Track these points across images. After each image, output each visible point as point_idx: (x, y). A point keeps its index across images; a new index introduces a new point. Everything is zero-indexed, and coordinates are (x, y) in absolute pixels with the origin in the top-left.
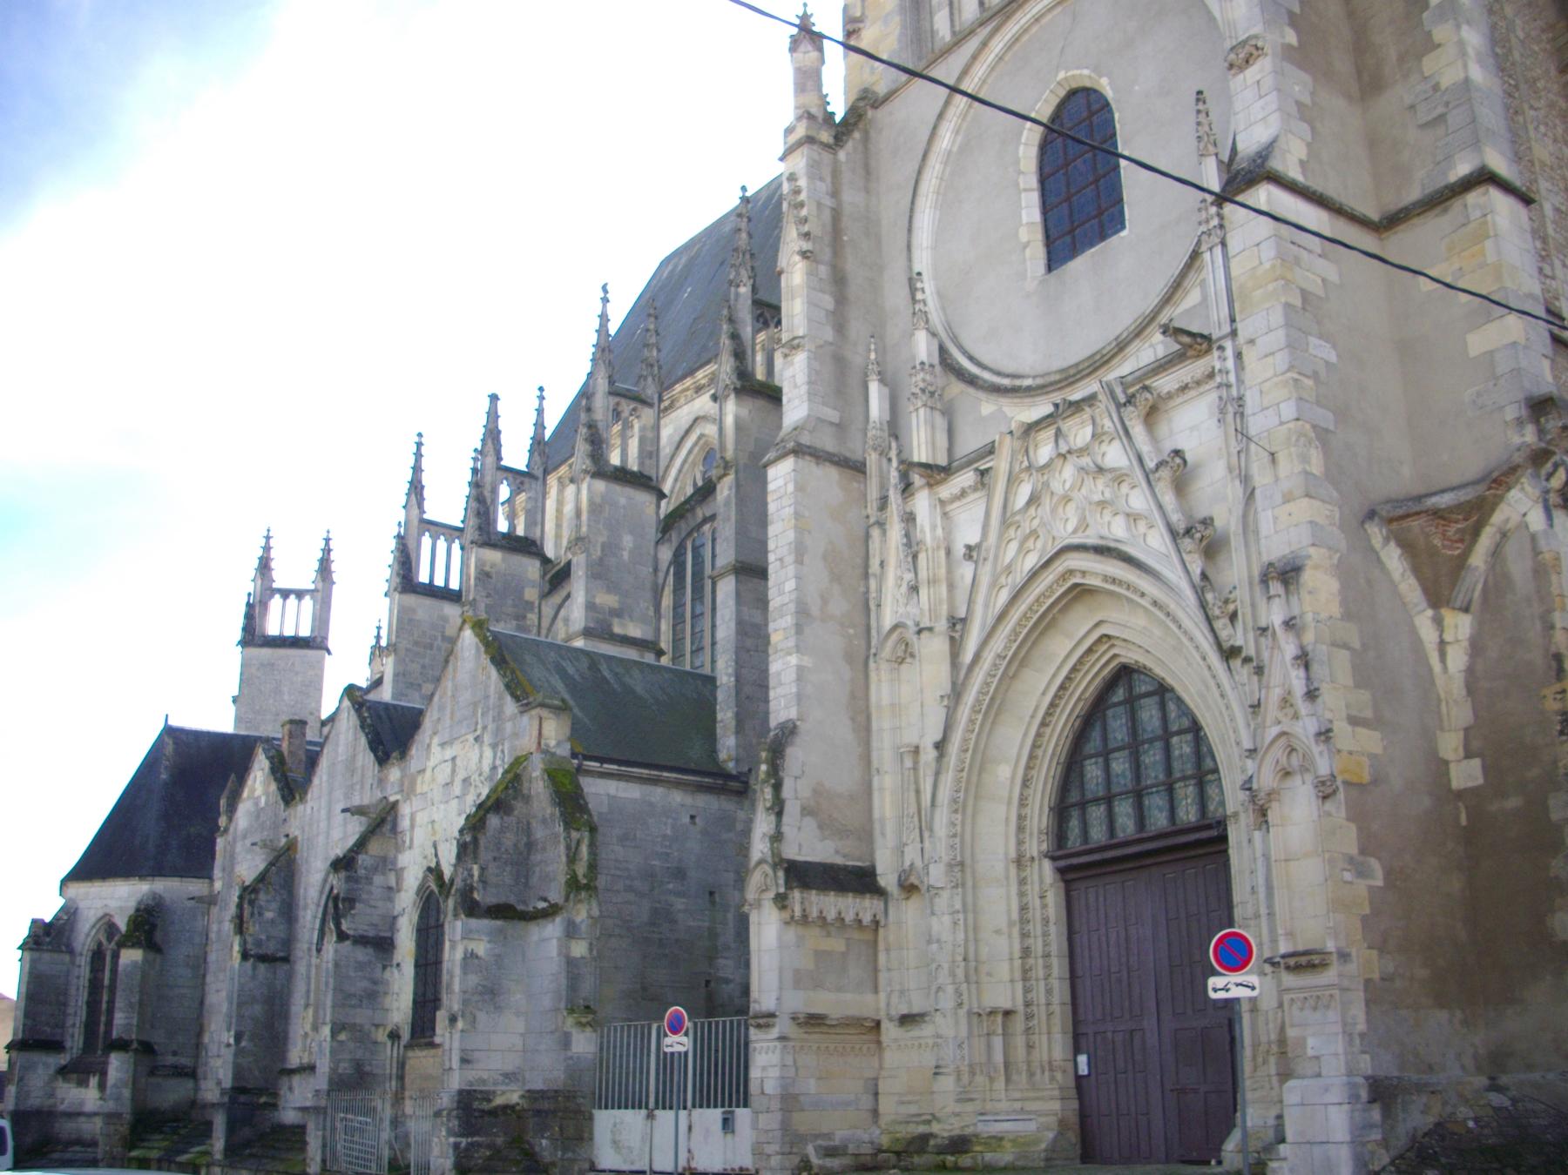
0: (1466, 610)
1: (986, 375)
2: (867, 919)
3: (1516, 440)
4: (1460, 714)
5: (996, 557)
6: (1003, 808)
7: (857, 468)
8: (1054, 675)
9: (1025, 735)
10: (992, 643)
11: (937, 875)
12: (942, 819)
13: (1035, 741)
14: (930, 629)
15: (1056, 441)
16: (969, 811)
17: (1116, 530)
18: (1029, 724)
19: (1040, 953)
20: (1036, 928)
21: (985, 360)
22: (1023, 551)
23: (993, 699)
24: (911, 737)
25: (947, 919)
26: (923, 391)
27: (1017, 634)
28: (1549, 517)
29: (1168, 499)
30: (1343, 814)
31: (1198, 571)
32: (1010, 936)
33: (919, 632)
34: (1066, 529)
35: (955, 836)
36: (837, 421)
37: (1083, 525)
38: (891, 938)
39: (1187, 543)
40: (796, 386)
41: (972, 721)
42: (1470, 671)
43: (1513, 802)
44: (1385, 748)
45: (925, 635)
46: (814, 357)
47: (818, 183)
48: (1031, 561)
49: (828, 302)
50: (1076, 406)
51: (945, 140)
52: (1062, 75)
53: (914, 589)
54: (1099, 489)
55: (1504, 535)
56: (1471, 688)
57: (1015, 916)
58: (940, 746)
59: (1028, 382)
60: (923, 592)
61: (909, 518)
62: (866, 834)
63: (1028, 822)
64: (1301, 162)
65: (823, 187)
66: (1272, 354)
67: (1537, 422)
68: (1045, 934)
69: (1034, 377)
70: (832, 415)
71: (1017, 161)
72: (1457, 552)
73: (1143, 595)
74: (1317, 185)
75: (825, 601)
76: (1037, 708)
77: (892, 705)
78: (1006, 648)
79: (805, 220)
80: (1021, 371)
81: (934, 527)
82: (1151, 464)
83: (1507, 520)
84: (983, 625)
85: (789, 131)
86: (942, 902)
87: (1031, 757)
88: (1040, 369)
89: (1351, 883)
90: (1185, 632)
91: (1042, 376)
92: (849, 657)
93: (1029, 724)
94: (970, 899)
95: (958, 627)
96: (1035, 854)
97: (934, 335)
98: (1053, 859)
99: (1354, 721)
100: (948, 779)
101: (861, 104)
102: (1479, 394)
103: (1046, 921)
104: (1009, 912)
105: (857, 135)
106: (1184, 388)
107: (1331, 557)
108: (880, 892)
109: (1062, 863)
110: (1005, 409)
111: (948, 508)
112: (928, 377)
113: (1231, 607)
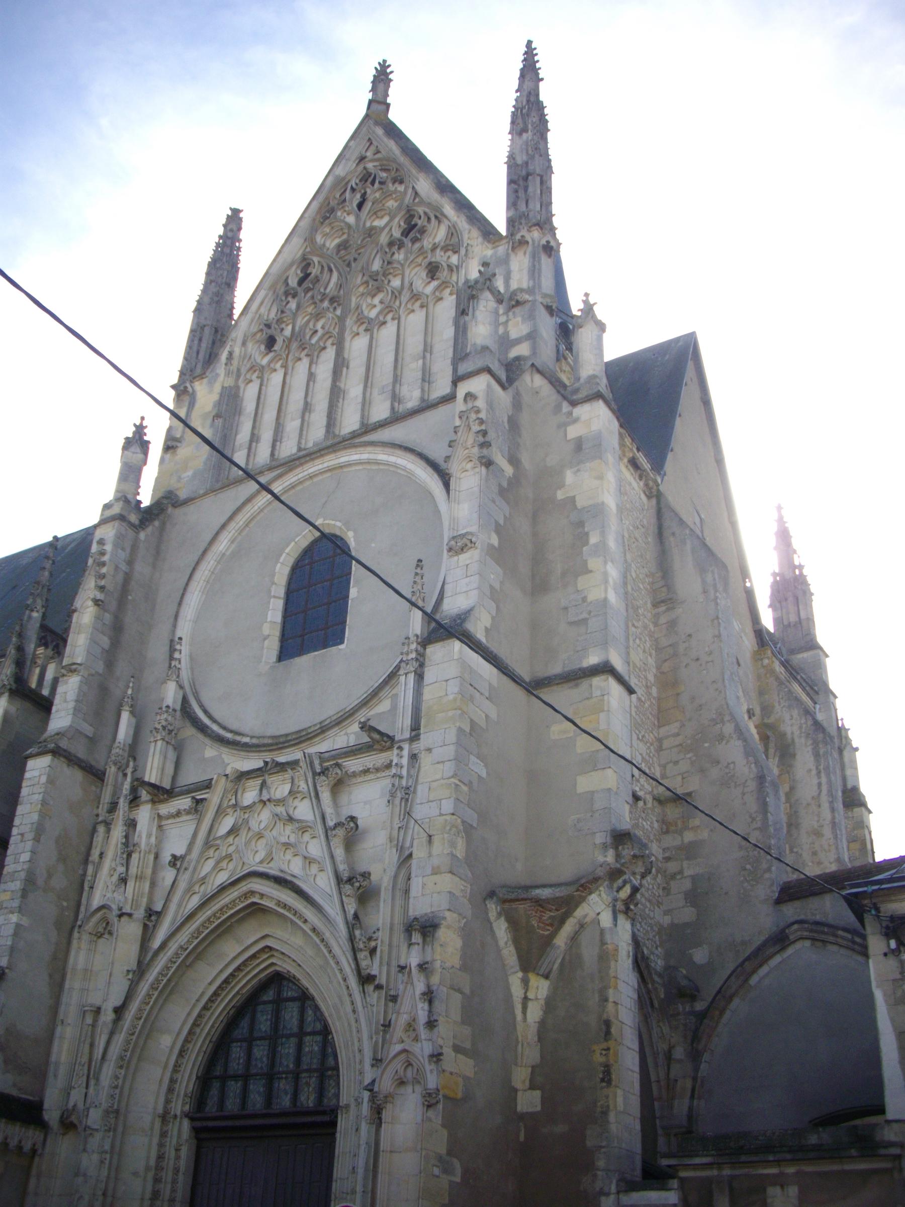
0: (546, 977)
1: (215, 727)
2: (27, 1147)
3: (601, 859)
4: (530, 1054)
5: (195, 869)
6: (159, 1071)
7: (97, 775)
8: (221, 971)
9: (189, 1014)
10: (178, 936)
11: (94, 1117)
12: (108, 1072)
13: (196, 1020)
14: (130, 915)
15: (261, 790)
16: (131, 1071)
17: (295, 867)
18: (194, 1006)
19: (167, 1197)
20: (167, 1175)
22: (217, 868)
23: (169, 980)
24: (95, 999)
25: (95, 1157)
26: (164, 728)
27: (199, 933)
28: (615, 919)
29: (339, 852)
30: (440, 1122)
31: (352, 912)
33: (120, 916)
34: (254, 859)
35: (116, 1087)
36: (91, 736)
37: (269, 858)
39: (347, 889)
40: (65, 701)
41: (149, 996)
42: (542, 1023)
43: (561, 1128)
44: (476, 1073)
45: (123, 919)
46: (85, 682)
47: (120, 551)
48: (222, 878)
49: (105, 642)
50: (282, 767)
51: (223, 545)
53: (123, 880)
54: (287, 833)
55: (582, 926)
56: (542, 1035)
57: (152, 1163)
58: (119, 1011)
59: (246, 740)
60: (131, 884)
61: (132, 824)
62: (41, 1073)
63: (177, 1086)
64: (486, 628)
65: (123, 555)
66: (443, 762)
67: (616, 848)
68: (174, 1181)
69: (252, 737)
70: (88, 730)
71: (273, 575)
72: (546, 933)
73: (306, 921)
74: (494, 647)
75: (50, 876)
76: (203, 993)
77: (86, 970)
79: (103, 577)
80: (242, 730)
81: (149, 836)
82: (331, 823)
83: (586, 916)
84: (174, 920)
85: (107, 507)
86: (94, 1142)
87: (191, 1032)
88: (258, 731)
89: (438, 1177)
90: (334, 957)
91: (258, 738)
92: (58, 925)
93: (194, 1006)
94: (118, 1144)
95: (153, 918)
96: (178, 1113)
97: (181, 687)
98: (192, 1119)
99: (457, 1049)
100: (120, 1039)
101: (165, 501)
102: (579, 820)
103: (176, 1171)
104: (148, 1158)
105: (157, 523)
106: (366, 771)
107: (459, 921)
108: (42, 1125)
109: (198, 1124)
110: (223, 756)
111: (163, 823)
112: (170, 718)
113: (373, 944)
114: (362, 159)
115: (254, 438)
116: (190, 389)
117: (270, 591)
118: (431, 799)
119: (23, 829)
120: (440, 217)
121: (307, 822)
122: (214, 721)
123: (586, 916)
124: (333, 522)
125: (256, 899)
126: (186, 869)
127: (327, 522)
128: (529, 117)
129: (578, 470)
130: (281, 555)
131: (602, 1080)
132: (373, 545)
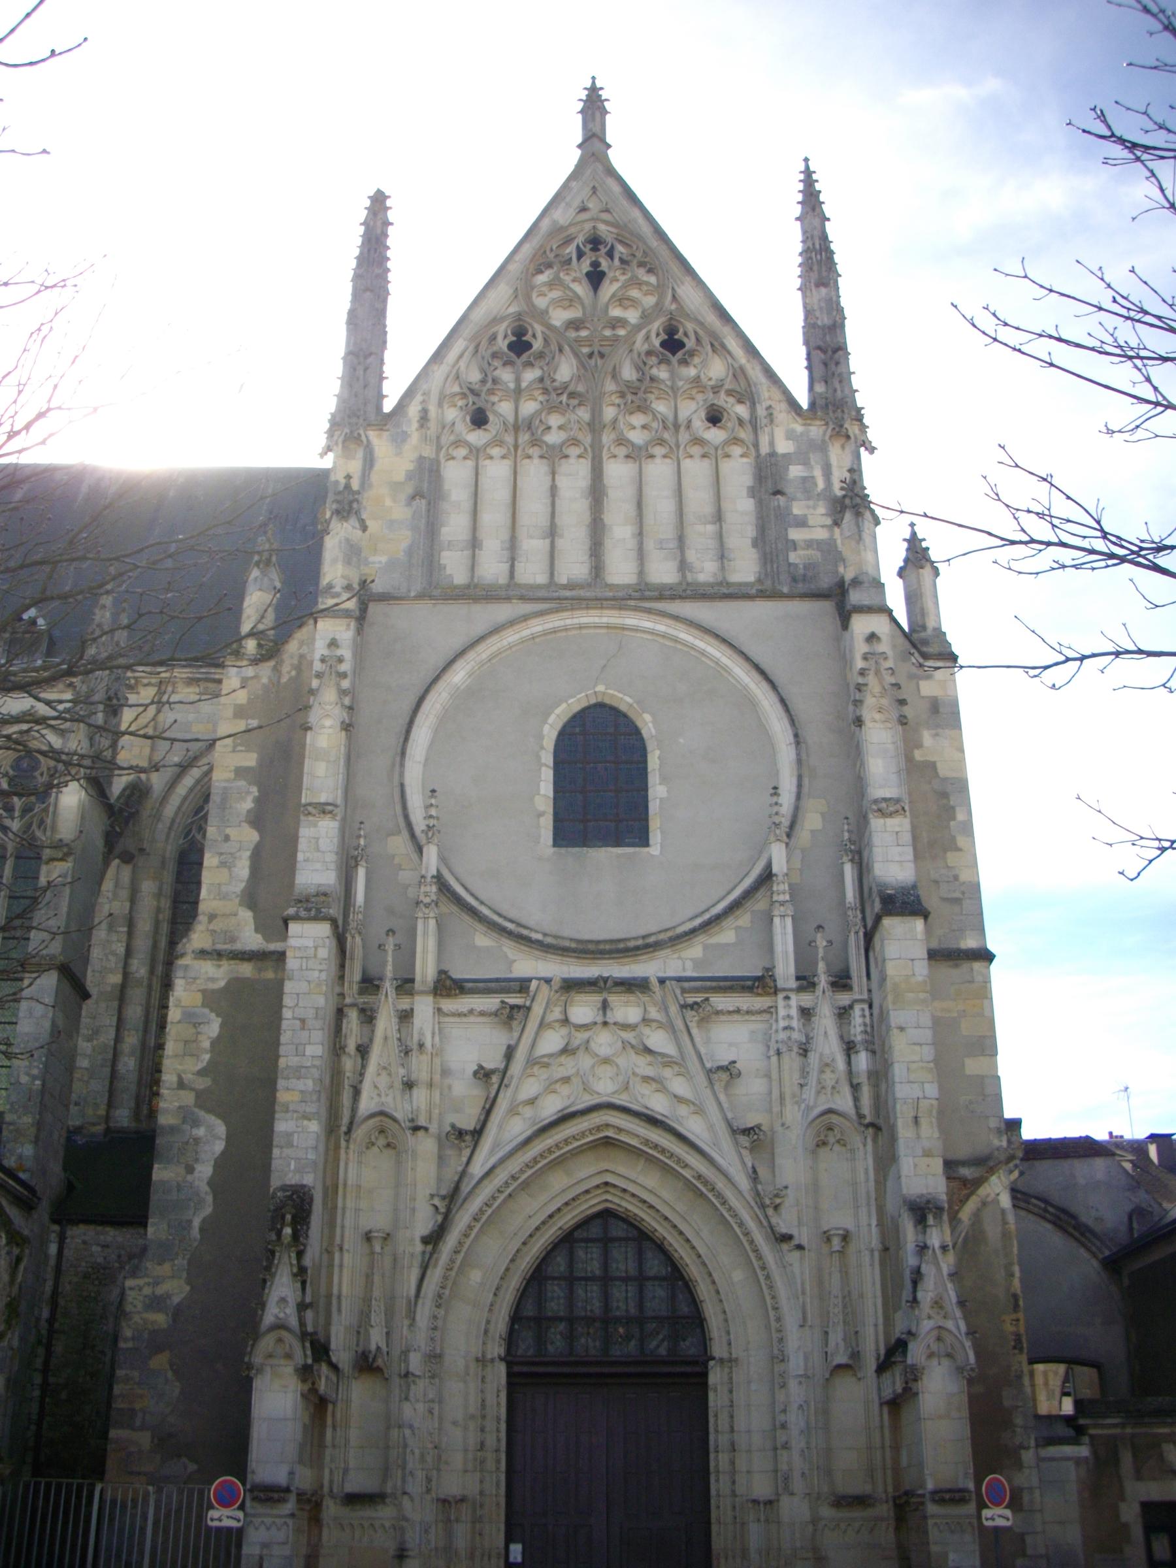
1: (485, 911)
3: (996, 1142)
11: (415, 1362)
14: (426, 1129)
17: (658, 1105)
21: (483, 897)
22: (550, 1089)
25: (420, 1407)
32: (466, 1428)
33: (416, 1129)
34: (605, 1087)
38: (338, 1415)
40: (318, 850)
41: (470, 1227)
45: (421, 1133)
51: (458, 676)
52: (600, 688)
53: (409, 1085)
54: (643, 1065)
55: (984, 1204)
69: (545, 935)
78: (522, 1171)
80: (524, 921)
83: (988, 1195)
90: (730, 1209)
102: (971, 1102)
106: (738, 1011)
109: (516, 1369)
113: (778, 1201)
114: (584, 209)
115: (474, 544)
116: (364, 438)
117: (538, 757)
118: (912, 1079)
119: (300, 1012)
120: (719, 347)
121: (671, 1057)
122: (482, 903)
123: (988, 1195)
124: (621, 695)
125: (610, 1133)
126: (506, 1086)
127: (611, 692)
128: (819, 264)
129: (937, 735)
130: (549, 715)
131: (1015, 1348)
132: (681, 740)
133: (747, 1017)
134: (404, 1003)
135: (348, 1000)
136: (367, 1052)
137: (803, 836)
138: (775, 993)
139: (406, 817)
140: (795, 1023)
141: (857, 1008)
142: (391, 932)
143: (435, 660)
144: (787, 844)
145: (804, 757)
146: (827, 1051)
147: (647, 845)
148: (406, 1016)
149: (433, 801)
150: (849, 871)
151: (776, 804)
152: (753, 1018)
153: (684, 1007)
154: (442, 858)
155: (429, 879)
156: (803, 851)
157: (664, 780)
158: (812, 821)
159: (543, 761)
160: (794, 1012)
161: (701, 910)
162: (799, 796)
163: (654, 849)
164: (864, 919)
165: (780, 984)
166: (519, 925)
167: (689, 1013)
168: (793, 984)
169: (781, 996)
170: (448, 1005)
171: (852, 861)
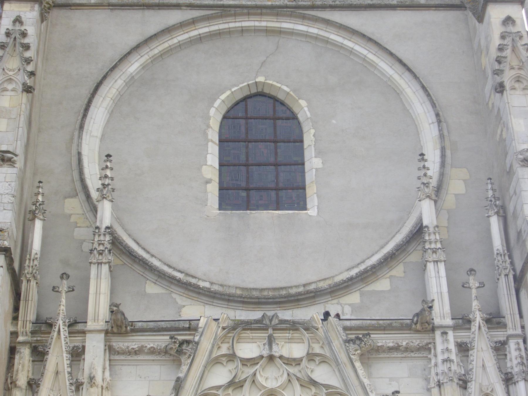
1: (156, 263)
51: (133, 66)
52: (261, 79)
69: (212, 283)
79: (28, 61)
80: (192, 272)
106: (396, 348)
117: (205, 134)
121: (336, 388)
122: (153, 256)
124: (279, 85)
127: (271, 82)
132: (334, 121)
133: (405, 354)
134: (77, 341)
135: (21, 339)
136: (38, 386)
137: (449, 200)
138: (433, 330)
139: (82, 180)
140: (453, 357)
141: (512, 344)
142: (64, 276)
143: (112, 55)
144: (436, 202)
145: (446, 133)
146: (485, 383)
147: (305, 208)
148: (77, 354)
149: (108, 164)
150: (495, 223)
151: (424, 167)
152: (412, 354)
153: (348, 341)
154: (116, 216)
155: (103, 230)
156: (449, 211)
157: (319, 153)
158: (456, 186)
159: (210, 137)
160: (452, 346)
161: (358, 261)
162: (443, 164)
163: (312, 211)
164: (512, 263)
165: (437, 321)
166: (187, 275)
167: (352, 346)
168: (449, 322)
169: (438, 333)
170: (120, 343)
171: (497, 213)
